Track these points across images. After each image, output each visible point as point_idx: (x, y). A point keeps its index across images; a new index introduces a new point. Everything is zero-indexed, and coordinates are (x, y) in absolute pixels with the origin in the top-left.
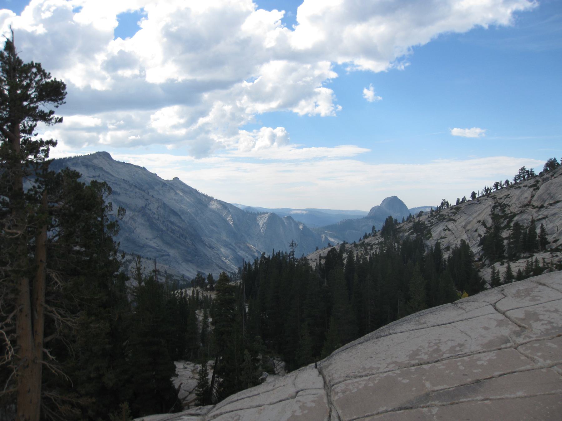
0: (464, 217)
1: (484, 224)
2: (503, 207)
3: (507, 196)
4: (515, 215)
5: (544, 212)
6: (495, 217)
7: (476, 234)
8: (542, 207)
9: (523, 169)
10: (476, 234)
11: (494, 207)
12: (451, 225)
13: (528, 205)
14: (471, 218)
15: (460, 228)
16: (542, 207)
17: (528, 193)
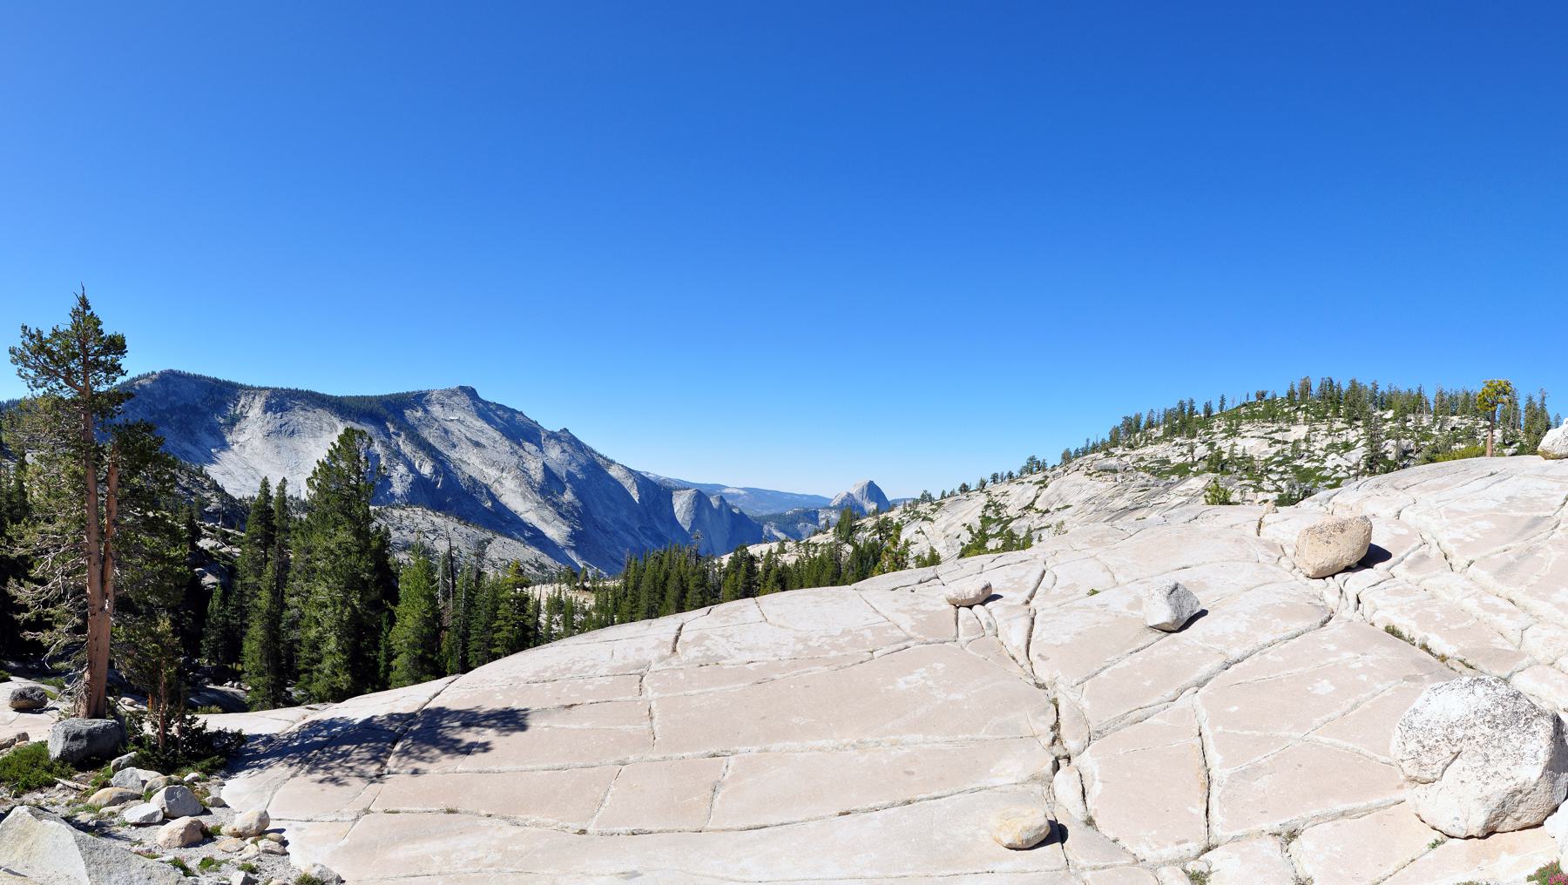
0: (946, 516)
1: (970, 528)
2: (999, 507)
3: (1005, 494)
4: (1012, 520)
5: (1048, 519)
6: (986, 520)
7: (958, 542)
8: (1047, 511)
9: (1032, 459)
10: (958, 542)
11: (987, 507)
12: (926, 526)
13: (1028, 508)
14: (954, 519)
15: (938, 532)
16: (1047, 511)
17: (1032, 491)
